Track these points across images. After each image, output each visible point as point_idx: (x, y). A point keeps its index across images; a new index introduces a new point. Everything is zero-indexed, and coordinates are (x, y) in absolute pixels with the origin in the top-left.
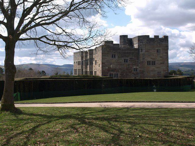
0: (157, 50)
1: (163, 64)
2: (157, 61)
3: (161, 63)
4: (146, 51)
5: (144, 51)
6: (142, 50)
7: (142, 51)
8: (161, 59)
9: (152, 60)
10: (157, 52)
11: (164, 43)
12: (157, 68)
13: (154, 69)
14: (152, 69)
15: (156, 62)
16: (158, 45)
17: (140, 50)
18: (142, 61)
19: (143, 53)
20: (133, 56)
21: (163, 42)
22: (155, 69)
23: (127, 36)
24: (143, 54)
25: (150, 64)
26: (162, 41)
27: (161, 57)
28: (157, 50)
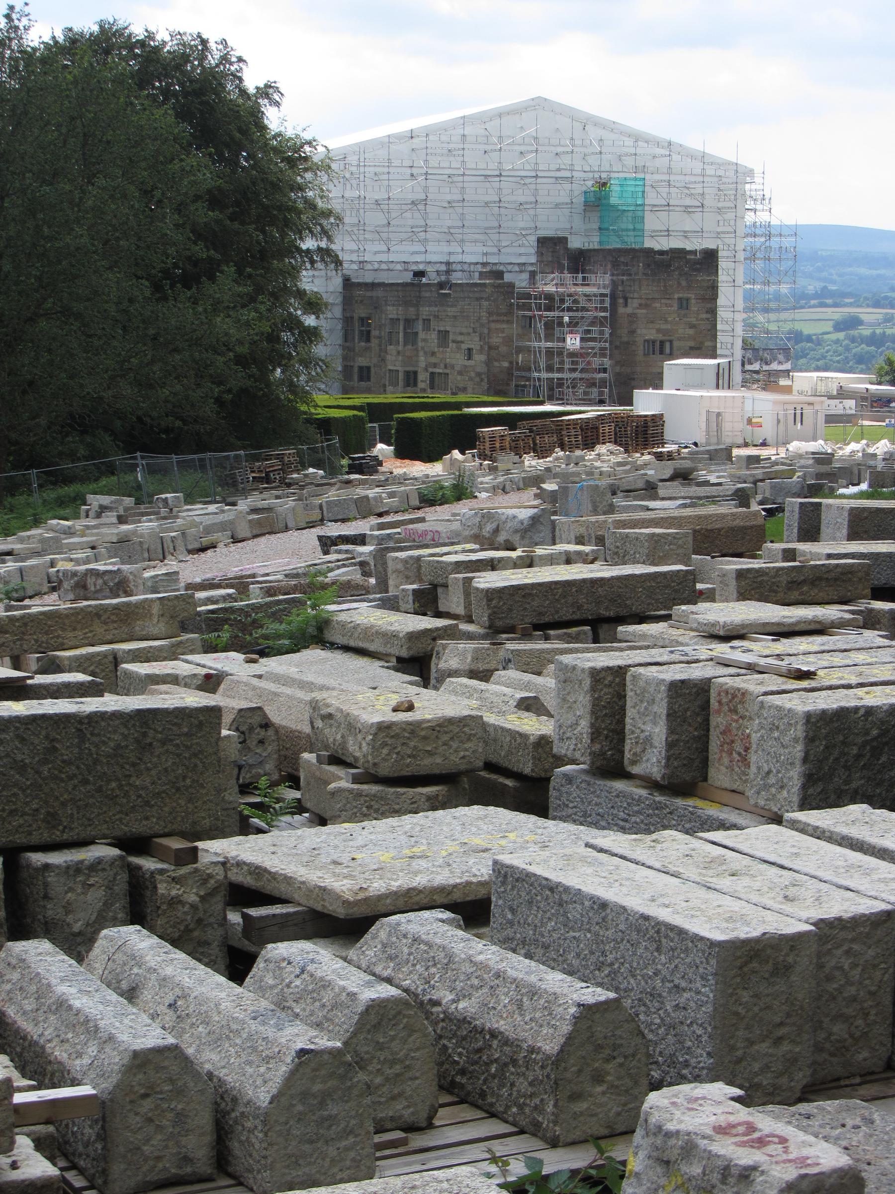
2: (679, 339)
3: (691, 348)
4: (640, 305)
6: (626, 299)
7: (626, 305)
8: (691, 332)
9: (660, 337)
10: (681, 307)
11: (702, 277)
16: (684, 283)
17: (621, 301)
18: (625, 339)
19: (629, 310)
23: (563, 240)
24: (629, 315)
27: (692, 326)
28: (680, 299)
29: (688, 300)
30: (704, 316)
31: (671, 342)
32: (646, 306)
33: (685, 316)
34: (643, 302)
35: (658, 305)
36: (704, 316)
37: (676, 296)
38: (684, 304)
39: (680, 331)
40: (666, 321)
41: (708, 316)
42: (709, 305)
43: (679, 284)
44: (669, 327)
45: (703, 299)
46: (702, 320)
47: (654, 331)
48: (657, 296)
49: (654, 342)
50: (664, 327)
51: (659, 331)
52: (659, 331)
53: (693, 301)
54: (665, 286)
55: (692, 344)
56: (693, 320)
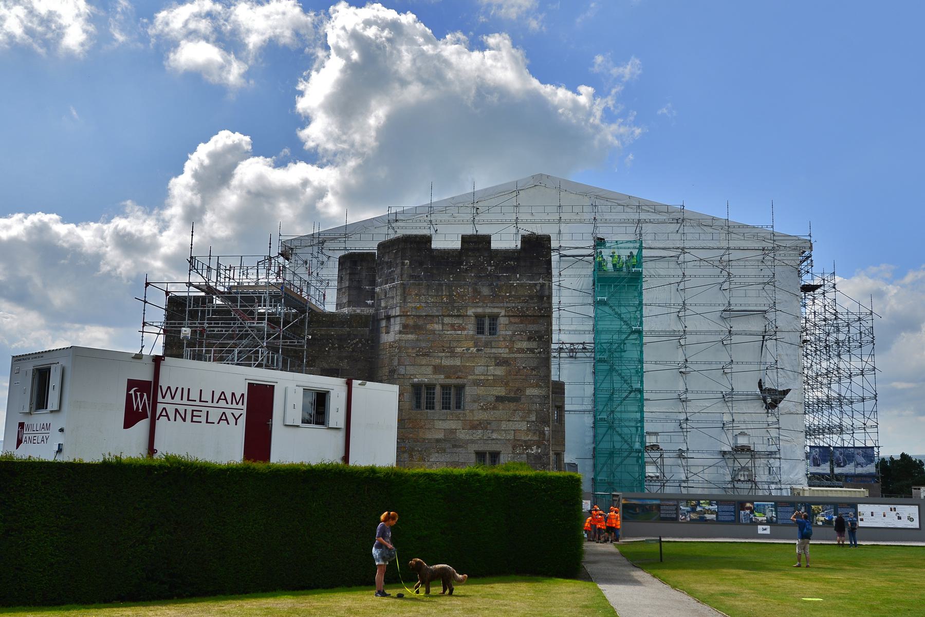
0: (479, 318)
1: (512, 405)
2: (476, 383)
3: (499, 399)
4: (405, 326)
5: (396, 326)
8: (500, 371)
9: (441, 379)
10: (480, 330)
12: (474, 427)
13: (453, 431)
14: (441, 436)
15: (469, 391)
16: (485, 291)
20: (341, 359)
21: (513, 270)
22: (463, 435)
25: (430, 406)
26: (507, 269)
27: (501, 362)
28: (479, 318)
29: (494, 318)
30: (525, 345)
31: (460, 388)
32: (416, 328)
33: (488, 344)
34: (411, 322)
35: (437, 327)
36: (525, 345)
37: (470, 312)
38: (486, 325)
39: (478, 370)
40: (453, 354)
41: (533, 345)
42: (533, 327)
43: (476, 291)
44: (458, 362)
45: (523, 317)
46: (521, 351)
47: (429, 370)
48: (435, 312)
49: (430, 387)
50: (447, 362)
51: (437, 369)
52: (437, 369)
53: (502, 321)
54: (450, 296)
55: (501, 391)
56: (503, 352)
